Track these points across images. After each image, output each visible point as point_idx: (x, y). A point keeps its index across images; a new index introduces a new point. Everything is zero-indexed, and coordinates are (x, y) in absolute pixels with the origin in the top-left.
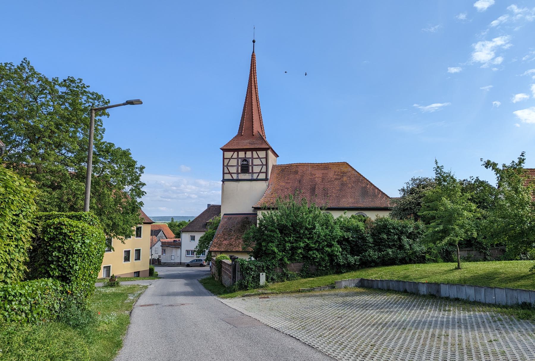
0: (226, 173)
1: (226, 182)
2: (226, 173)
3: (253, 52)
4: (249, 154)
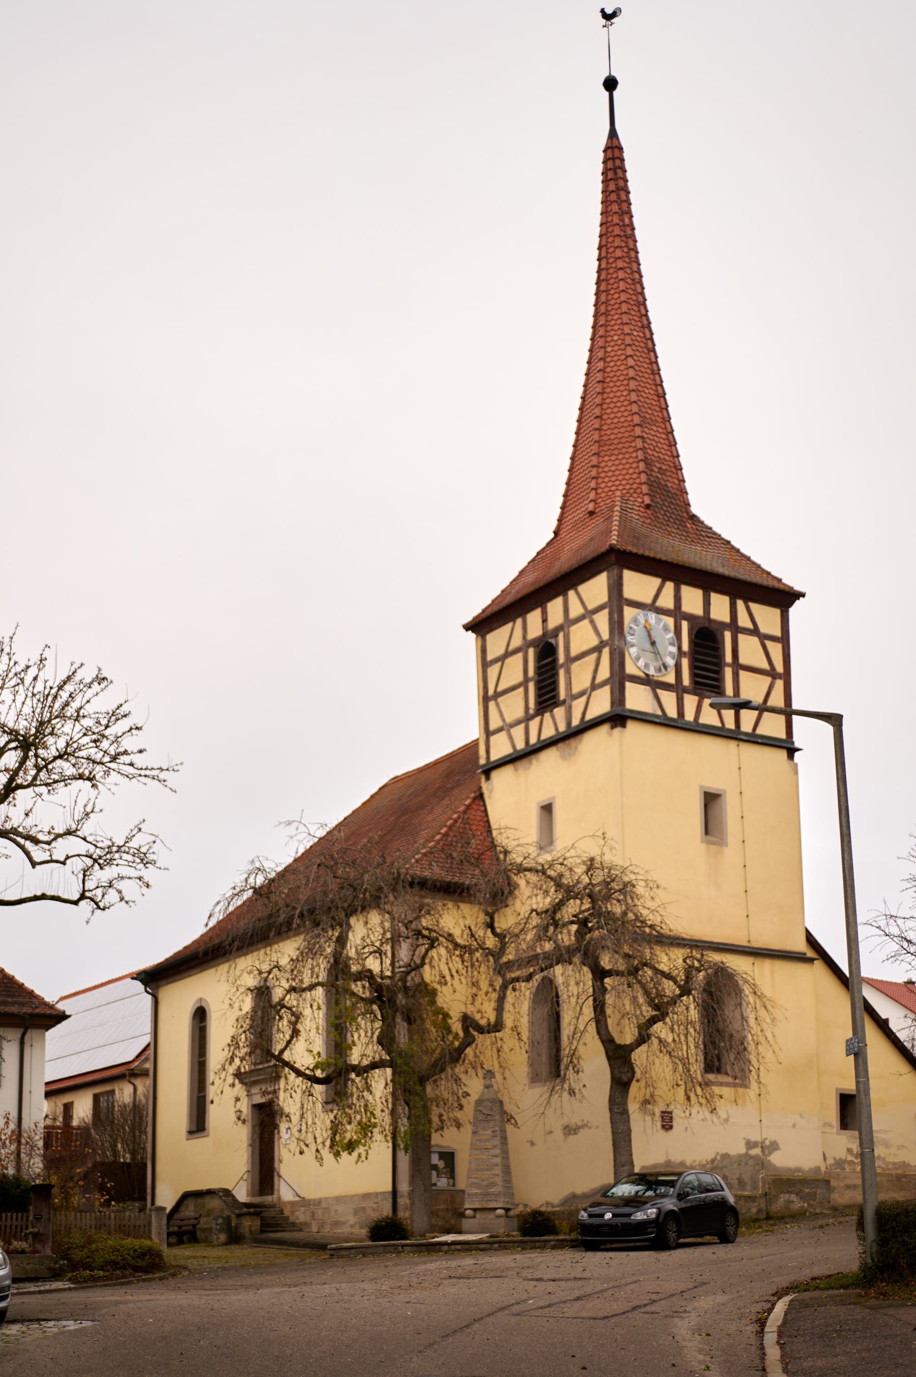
3: (613, 134)
4: (720, 608)
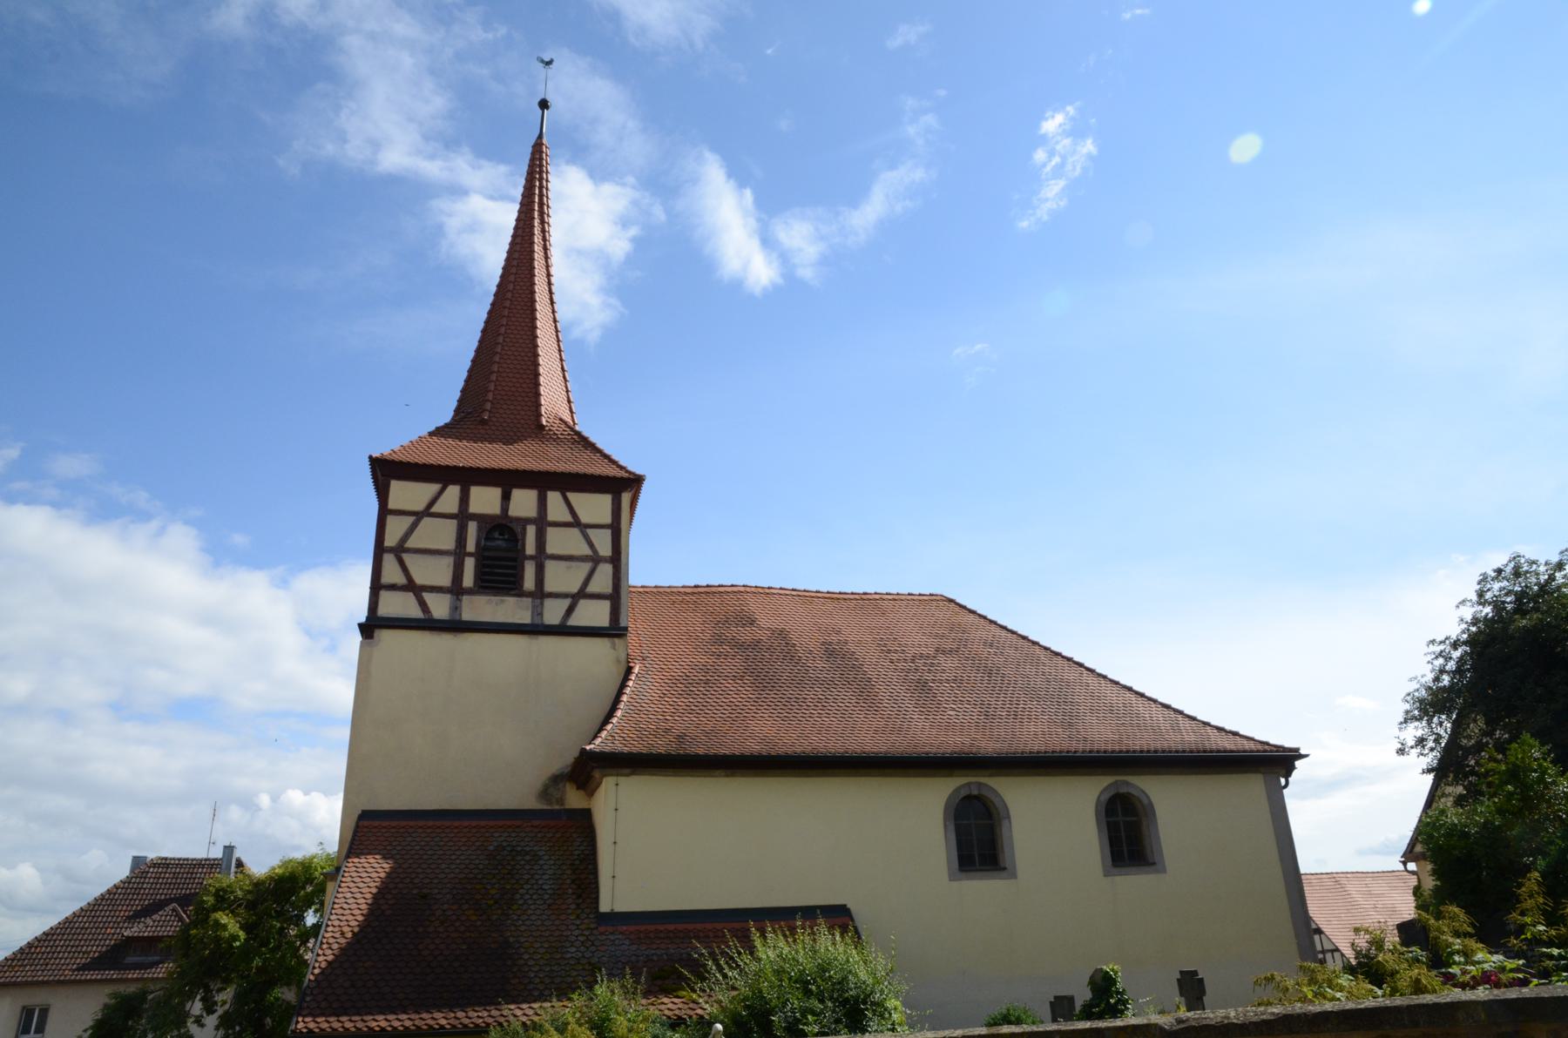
0: (393, 587)
1: (385, 636)
2: (393, 587)
4: (524, 502)
